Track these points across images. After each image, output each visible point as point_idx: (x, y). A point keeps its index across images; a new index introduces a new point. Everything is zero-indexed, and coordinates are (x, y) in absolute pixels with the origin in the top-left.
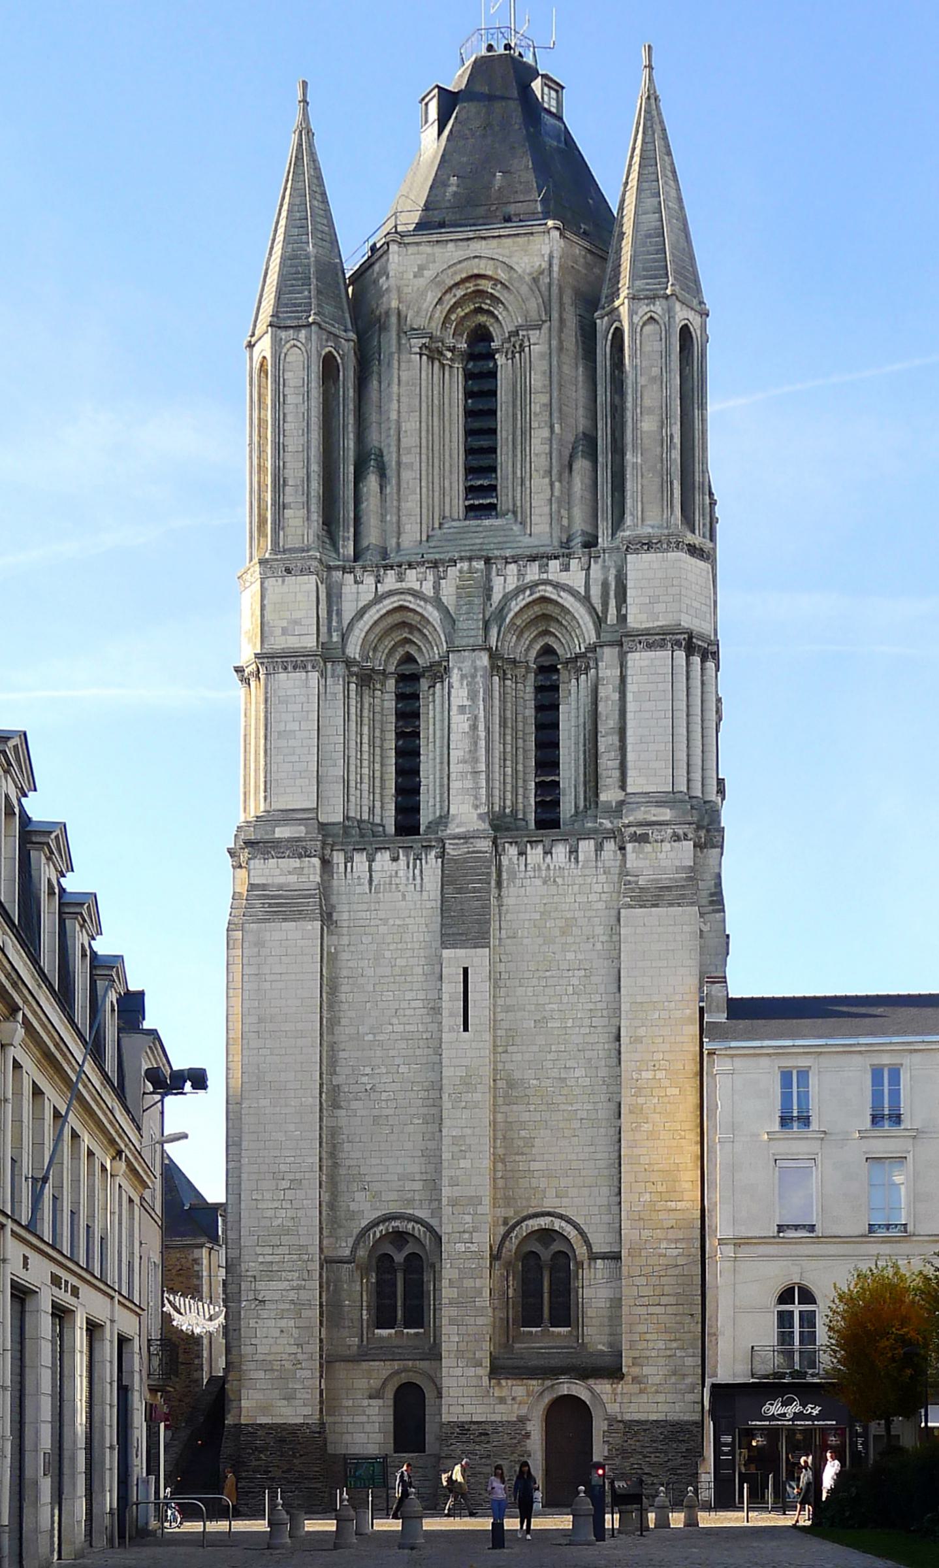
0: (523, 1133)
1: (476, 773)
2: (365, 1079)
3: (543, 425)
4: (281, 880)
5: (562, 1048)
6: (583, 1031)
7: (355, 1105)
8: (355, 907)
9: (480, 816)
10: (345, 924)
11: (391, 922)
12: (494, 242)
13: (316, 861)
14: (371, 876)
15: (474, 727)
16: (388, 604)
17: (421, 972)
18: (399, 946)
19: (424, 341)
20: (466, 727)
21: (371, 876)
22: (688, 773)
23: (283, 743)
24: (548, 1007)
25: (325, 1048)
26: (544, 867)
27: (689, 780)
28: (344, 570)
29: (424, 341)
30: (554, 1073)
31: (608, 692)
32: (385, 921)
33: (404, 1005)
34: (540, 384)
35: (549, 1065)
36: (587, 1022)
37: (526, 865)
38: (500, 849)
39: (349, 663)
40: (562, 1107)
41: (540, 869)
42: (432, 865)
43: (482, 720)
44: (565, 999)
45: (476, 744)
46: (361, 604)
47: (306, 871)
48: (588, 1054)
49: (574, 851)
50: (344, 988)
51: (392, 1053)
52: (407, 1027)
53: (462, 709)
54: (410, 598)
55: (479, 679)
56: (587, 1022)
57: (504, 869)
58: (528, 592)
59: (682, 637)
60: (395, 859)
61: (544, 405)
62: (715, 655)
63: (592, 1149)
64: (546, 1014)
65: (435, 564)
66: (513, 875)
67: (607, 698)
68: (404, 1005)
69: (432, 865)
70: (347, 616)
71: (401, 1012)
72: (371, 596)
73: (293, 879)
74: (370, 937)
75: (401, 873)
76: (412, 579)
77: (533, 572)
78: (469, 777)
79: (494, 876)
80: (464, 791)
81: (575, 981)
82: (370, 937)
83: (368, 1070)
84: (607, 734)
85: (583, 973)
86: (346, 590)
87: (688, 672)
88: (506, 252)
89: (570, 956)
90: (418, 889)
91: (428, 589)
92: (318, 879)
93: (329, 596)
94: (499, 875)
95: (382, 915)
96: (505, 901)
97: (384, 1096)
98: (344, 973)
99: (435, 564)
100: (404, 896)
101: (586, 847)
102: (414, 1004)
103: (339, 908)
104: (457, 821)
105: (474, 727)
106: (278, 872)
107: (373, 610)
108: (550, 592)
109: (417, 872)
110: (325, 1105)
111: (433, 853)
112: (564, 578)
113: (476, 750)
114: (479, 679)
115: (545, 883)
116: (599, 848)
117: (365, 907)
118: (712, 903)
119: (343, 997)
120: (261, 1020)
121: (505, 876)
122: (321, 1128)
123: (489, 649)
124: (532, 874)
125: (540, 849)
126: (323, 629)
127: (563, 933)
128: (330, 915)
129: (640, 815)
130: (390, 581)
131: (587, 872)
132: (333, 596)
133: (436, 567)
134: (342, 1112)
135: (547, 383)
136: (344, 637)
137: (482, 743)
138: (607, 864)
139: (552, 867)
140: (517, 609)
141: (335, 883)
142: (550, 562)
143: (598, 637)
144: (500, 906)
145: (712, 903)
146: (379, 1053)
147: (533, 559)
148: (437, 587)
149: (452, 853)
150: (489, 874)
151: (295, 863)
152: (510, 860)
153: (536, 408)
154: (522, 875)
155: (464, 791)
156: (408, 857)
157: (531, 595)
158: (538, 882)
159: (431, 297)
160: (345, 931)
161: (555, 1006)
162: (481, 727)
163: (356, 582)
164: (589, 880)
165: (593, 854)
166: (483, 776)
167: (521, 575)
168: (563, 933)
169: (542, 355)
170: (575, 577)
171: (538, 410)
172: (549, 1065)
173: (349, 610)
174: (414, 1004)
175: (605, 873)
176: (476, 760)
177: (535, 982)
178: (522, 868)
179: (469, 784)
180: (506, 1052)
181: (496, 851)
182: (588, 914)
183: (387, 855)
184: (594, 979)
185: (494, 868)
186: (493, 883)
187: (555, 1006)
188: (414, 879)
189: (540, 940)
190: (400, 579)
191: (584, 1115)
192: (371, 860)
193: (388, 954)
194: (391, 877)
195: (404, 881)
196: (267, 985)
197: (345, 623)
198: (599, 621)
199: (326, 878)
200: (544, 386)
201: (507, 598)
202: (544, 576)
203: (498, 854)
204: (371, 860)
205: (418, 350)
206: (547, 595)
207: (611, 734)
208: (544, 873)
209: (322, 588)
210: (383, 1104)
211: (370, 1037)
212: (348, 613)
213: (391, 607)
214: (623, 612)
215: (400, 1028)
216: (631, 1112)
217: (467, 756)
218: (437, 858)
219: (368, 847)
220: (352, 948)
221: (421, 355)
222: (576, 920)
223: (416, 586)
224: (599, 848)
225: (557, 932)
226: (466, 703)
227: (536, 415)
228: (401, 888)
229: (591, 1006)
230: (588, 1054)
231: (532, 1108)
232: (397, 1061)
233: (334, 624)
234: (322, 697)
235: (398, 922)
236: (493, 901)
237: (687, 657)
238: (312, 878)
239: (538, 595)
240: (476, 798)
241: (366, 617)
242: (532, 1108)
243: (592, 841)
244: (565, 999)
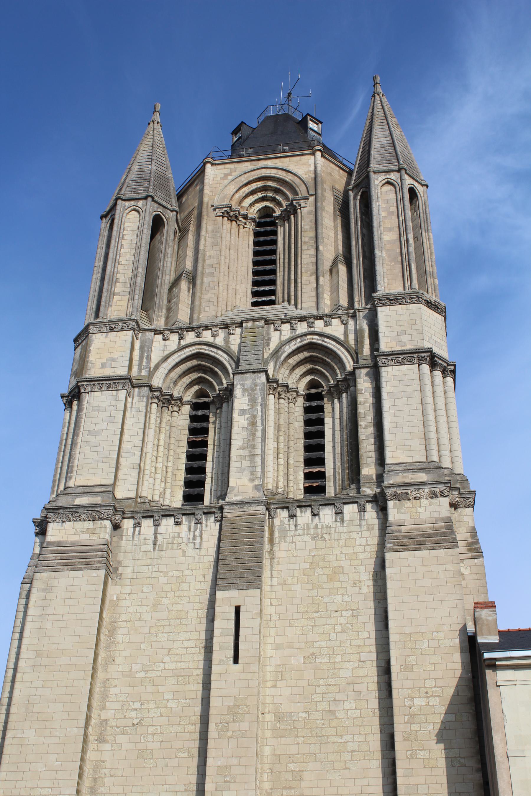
0: (291, 766)
1: (253, 456)
2: (133, 714)
3: (310, 247)
4: (75, 538)
5: (331, 682)
6: (351, 665)
7: (121, 739)
8: (139, 562)
9: (256, 487)
10: (129, 576)
11: (171, 574)
12: (277, 160)
13: (108, 523)
14: (155, 538)
15: (253, 424)
16: (188, 352)
17: (195, 615)
18: (177, 594)
19: (226, 209)
20: (246, 423)
21: (155, 538)
22: (439, 451)
23: (91, 438)
24: (317, 645)
25: (98, 684)
26: (312, 526)
27: (440, 457)
28: (157, 332)
29: (226, 209)
30: (324, 706)
31: (365, 400)
32: (165, 573)
33: (178, 644)
34: (307, 227)
35: (318, 698)
36: (355, 657)
37: (296, 526)
38: (272, 513)
39: (151, 389)
40: (332, 739)
41: (308, 528)
42: (211, 527)
43: (260, 418)
44: (333, 637)
45: (254, 435)
46: (167, 353)
47: (97, 531)
48: (357, 687)
49: (339, 513)
50: (122, 631)
51: (162, 689)
52: (179, 665)
53: (243, 412)
54: (205, 347)
55: (258, 391)
56: (355, 657)
57: (276, 529)
58: (299, 340)
59: (427, 354)
60: (177, 524)
61: (311, 237)
62: (453, 372)
63: (365, 782)
64: (315, 651)
65: (226, 326)
66: (284, 533)
67: (365, 402)
68: (178, 644)
69: (211, 527)
70: (155, 360)
71: (173, 651)
72: (175, 347)
73: (85, 538)
74: (150, 588)
75: (183, 535)
76: (207, 336)
77: (302, 327)
78: (247, 458)
79: (267, 535)
80: (242, 469)
81: (343, 621)
82: (150, 588)
83: (137, 705)
84: (366, 427)
85: (350, 613)
86: (154, 344)
87: (432, 382)
88: (286, 164)
89: (339, 598)
90: (197, 546)
91: (220, 341)
92: (107, 537)
93: (142, 348)
94: (272, 534)
95: (163, 568)
96: (277, 554)
97: (151, 730)
98: (124, 617)
99: (226, 326)
100: (184, 554)
101: (350, 510)
102: (186, 644)
103: (125, 563)
104: (236, 491)
105: (253, 424)
106: (73, 532)
107: (176, 355)
108: (316, 339)
109: (197, 533)
110: (91, 739)
111: (212, 518)
112: (327, 330)
113: (254, 439)
114: (258, 391)
115: (313, 538)
116: (362, 510)
117: (149, 562)
118: (470, 551)
119: (119, 638)
120: (38, 655)
121: (276, 534)
122: (82, 759)
123: (266, 372)
124: (301, 532)
125: (309, 511)
126: (135, 368)
127: (331, 580)
128: (116, 569)
129: (399, 478)
130: (190, 337)
131: (352, 529)
132: (146, 348)
133: (227, 328)
134: (107, 747)
135: (314, 226)
136: (151, 374)
137: (259, 435)
138: (370, 522)
139: (320, 526)
140: (290, 350)
141: (123, 543)
142: (316, 322)
143: (356, 360)
144: (272, 558)
145: (470, 551)
146: (150, 689)
147: (302, 319)
148: (227, 341)
149: (229, 515)
150: (262, 531)
151: (90, 525)
152: (281, 521)
153: (305, 239)
154: (292, 533)
155: (242, 469)
156: (190, 522)
157: (301, 341)
158: (307, 538)
159: (232, 189)
160: (128, 582)
161: (324, 644)
162: (259, 423)
163: (164, 339)
164: (354, 535)
165: (357, 515)
166: (259, 458)
167: (293, 328)
168: (331, 580)
169: (309, 213)
170: (336, 328)
171: (306, 240)
172: (318, 698)
173: (156, 356)
174: (186, 644)
175: (368, 529)
176: (254, 447)
177: (304, 622)
178: (293, 527)
179: (246, 463)
180: (275, 686)
181: (270, 515)
182: (354, 563)
183: (171, 520)
184: (361, 619)
185: (267, 529)
186: (266, 540)
187: (324, 644)
188: (194, 539)
189: (309, 586)
190: (198, 336)
191: (355, 747)
192: (157, 525)
193: (165, 601)
194: (174, 538)
195: (185, 540)
196: (49, 625)
197: (153, 365)
198: (356, 355)
199: (115, 539)
200: (311, 228)
201: (283, 344)
202: (312, 329)
203: (271, 517)
204: (157, 525)
205: (221, 214)
206: (314, 341)
207: (370, 427)
208: (312, 531)
209: (137, 344)
210: (150, 738)
211: (142, 674)
212: (156, 356)
213: (190, 353)
214: (376, 346)
215: (172, 666)
216: (404, 740)
217: (246, 444)
218: (216, 521)
219: (155, 515)
220: (133, 596)
221: (223, 217)
222: (343, 567)
223: (210, 340)
224: (362, 510)
225: (324, 578)
226: (247, 407)
227: (305, 243)
228: (183, 546)
229: (359, 642)
230: (357, 687)
231: (301, 740)
232: (167, 696)
233: (144, 364)
234: (128, 410)
235: (177, 573)
236: (266, 555)
237: (431, 371)
238: (102, 536)
239: (306, 342)
240: (252, 474)
241: (170, 360)
242: (301, 740)
243: (355, 506)
244: (333, 637)
